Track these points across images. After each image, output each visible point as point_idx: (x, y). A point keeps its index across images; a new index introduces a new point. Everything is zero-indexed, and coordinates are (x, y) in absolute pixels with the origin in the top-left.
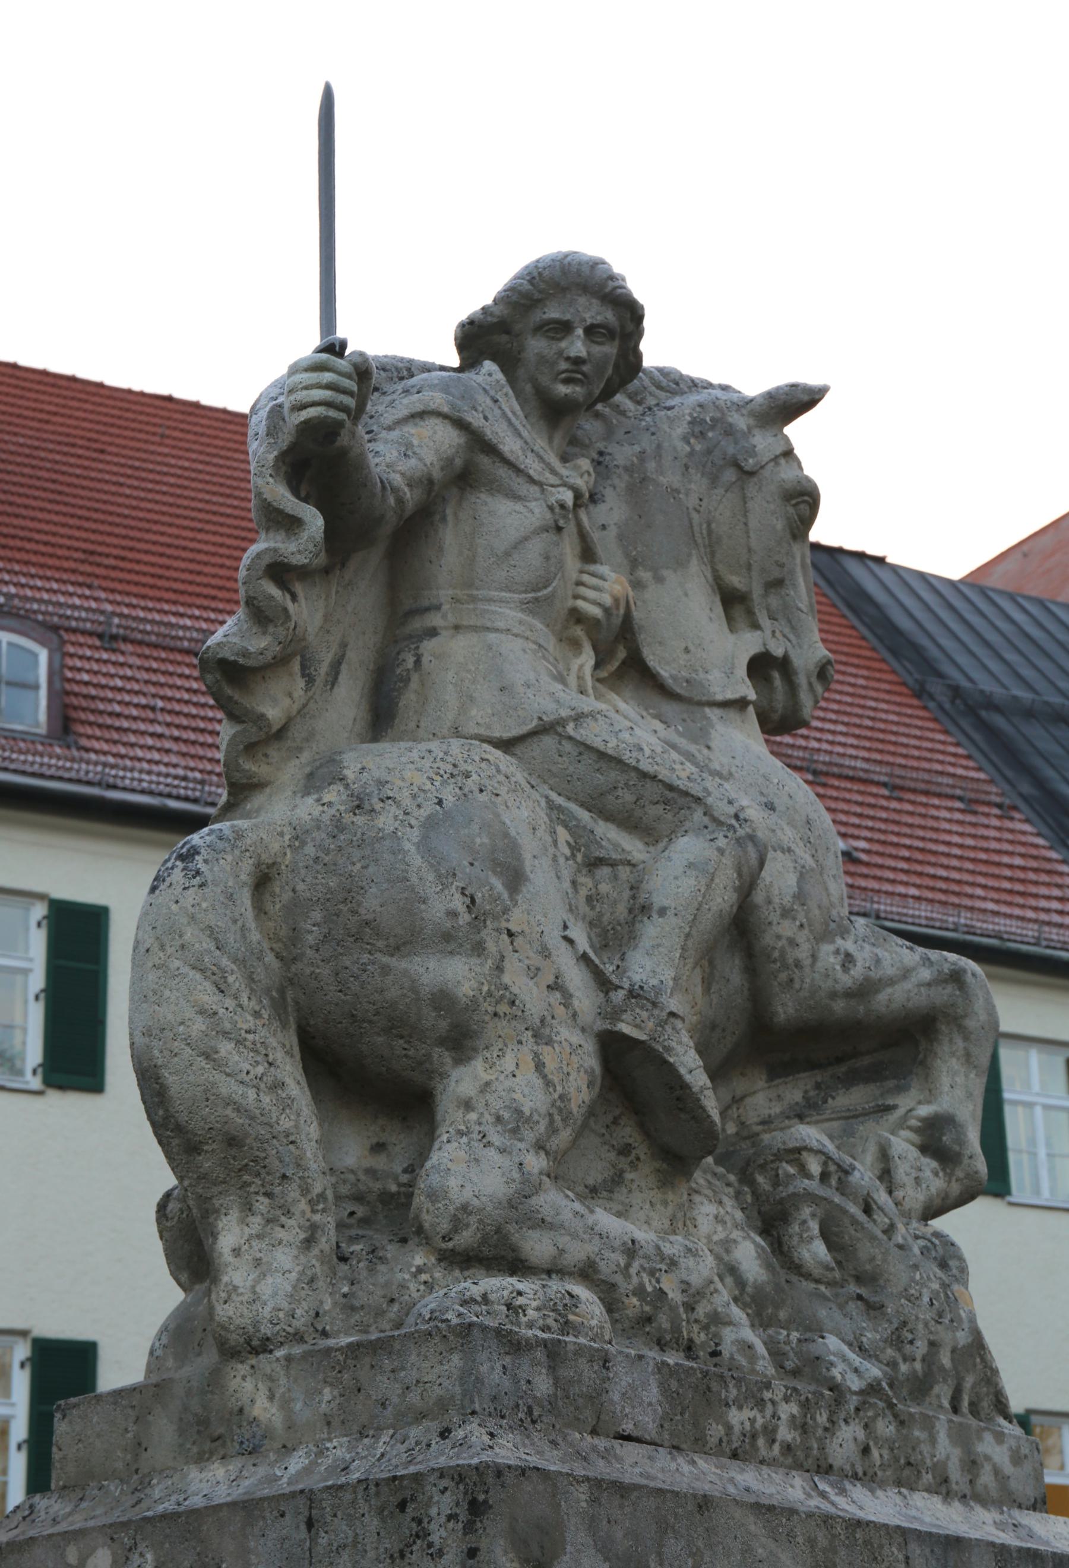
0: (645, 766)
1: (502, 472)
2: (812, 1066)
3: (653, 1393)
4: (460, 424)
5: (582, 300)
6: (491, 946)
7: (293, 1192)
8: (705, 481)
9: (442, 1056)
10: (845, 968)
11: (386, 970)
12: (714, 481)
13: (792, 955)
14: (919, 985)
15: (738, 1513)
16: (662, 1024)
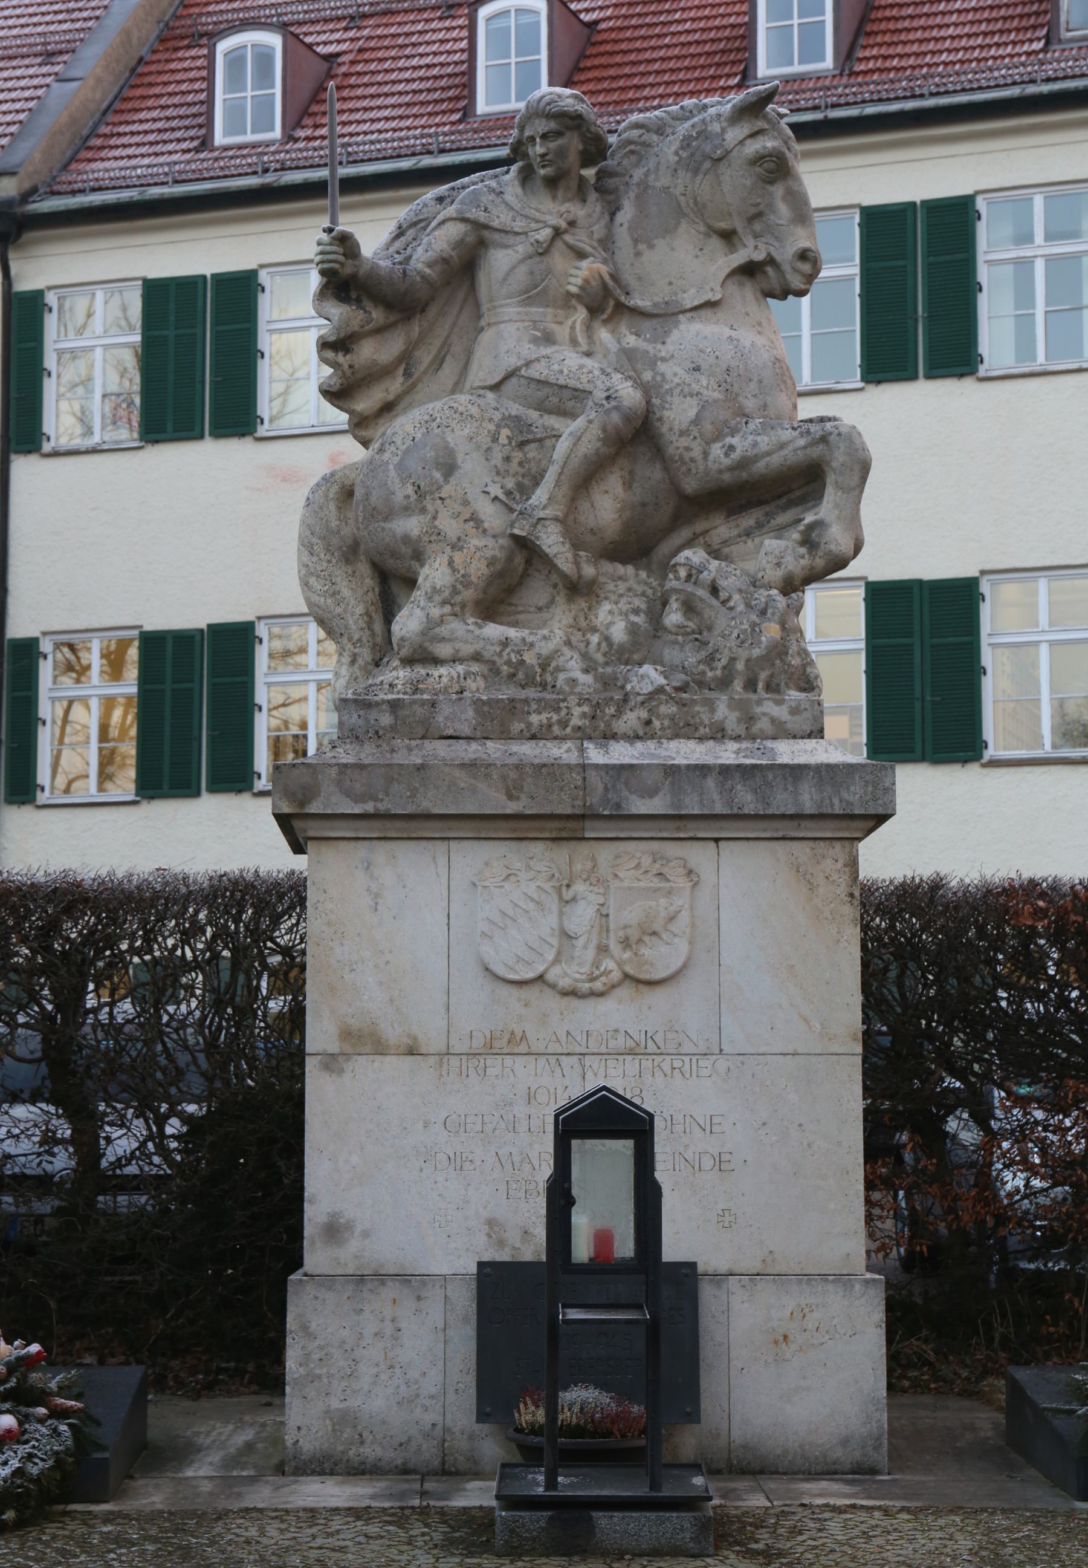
0: (561, 382)
1: (496, 236)
2: (760, 503)
3: (470, 713)
5: (537, 121)
6: (430, 508)
7: (345, 640)
8: (689, 174)
9: (415, 564)
10: (726, 455)
11: (383, 529)
12: (696, 171)
13: (687, 456)
14: (795, 450)
15: (447, 769)
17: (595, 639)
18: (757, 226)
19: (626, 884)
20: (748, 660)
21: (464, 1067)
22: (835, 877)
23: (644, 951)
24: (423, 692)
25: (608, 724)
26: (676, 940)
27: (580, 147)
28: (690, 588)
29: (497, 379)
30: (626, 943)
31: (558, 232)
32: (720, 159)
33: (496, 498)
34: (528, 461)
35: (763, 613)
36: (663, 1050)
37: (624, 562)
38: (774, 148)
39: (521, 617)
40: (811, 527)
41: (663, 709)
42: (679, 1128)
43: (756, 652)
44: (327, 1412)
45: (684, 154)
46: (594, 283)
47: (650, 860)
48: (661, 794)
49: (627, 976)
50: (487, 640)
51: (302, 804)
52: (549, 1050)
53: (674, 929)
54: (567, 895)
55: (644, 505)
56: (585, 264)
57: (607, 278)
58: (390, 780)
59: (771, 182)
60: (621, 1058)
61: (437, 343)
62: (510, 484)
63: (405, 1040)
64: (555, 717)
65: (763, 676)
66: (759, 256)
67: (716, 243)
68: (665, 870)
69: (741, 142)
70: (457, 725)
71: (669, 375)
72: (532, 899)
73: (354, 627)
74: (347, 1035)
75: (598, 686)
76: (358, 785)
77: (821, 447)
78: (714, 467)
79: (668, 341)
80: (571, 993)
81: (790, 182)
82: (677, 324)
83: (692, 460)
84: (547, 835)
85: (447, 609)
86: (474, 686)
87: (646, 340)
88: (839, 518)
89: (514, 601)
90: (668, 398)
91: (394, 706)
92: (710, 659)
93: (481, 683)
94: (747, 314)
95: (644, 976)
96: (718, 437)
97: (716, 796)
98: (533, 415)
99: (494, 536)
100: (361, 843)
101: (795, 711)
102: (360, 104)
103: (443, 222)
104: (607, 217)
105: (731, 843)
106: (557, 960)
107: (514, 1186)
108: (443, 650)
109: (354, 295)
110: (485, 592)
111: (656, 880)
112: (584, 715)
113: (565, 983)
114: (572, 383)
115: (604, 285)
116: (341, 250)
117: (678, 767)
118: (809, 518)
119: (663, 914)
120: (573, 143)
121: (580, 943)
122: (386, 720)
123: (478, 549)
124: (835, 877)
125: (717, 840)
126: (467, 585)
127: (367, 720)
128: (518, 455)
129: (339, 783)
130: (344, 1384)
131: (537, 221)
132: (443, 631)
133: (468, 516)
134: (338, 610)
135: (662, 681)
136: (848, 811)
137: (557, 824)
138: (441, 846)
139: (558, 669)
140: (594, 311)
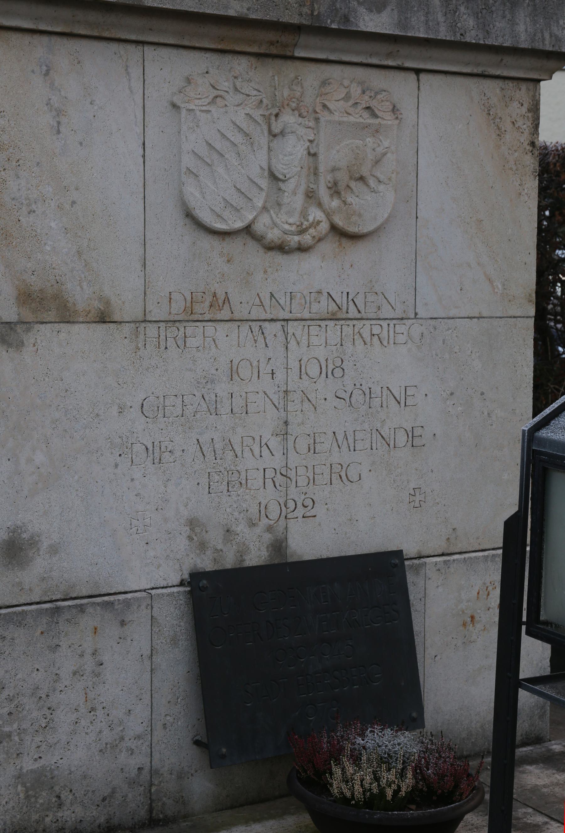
19: (336, 117)
21: (162, 337)
26: (381, 187)
36: (364, 315)
42: (376, 402)
44: (19, 776)
47: (359, 91)
48: (389, 9)
49: (334, 228)
52: (253, 316)
53: (379, 175)
60: (323, 323)
63: (96, 304)
68: (373, 104)
72: (240, 129)
84: (255, 49)
95: (352, 229)
97: (441, 19)
100: (37, 39)
107: (217, 478)
111: (366, 114)
113: (273, 235)
119: (371, 156)
125: (418, 72)
130: (38, 739)
137: (271, 36)
138: (134, 52)
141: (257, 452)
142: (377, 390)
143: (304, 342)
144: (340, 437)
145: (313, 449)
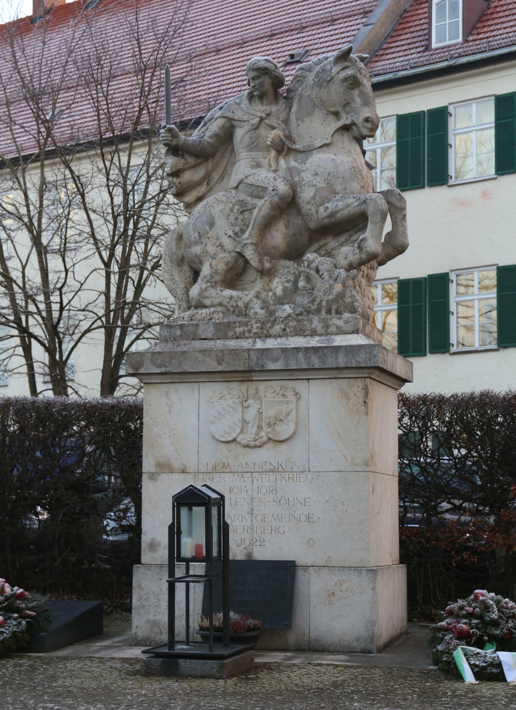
0: (258, 184)
2: (347, 231)
3: (212, 328)
4: (224, 117)
6: (204, 242)
10: (325, 211)
12: (321, 87)
13: (310, 213)
15: (194, 353)
16: (243, 247)
17: (270, 294)
18: (348, 109)
19: (269, 399)
20: (327, 301)
22: (358, 394)
23: (277, 428)
24: (194, 320)
25: (268, 331)
26: (290, 423)
27: (270, 81)
28: (308, 270)
29: (236, 185)
30: (269, 425)
31: (262, 119)
32: (329, 81)
33: (230, 236)
34: (245, 219)
35: (336, 280)
37: (290, 260)
38: (351, 74)
39: (246, 286)
40: (362, 241)
41: (291, 324)
43: (331, 297)
44: (148, 621)
45: (316, 80)
46: (277, 140)
47: (279, 389)
49: (270, 439)
50: (224, 297)
51: (137, 369)
52: (239, 471)
54: (245, 405)
55: (295, 235)
56: (273, 132)
57: (282, 137)
58: (171, 358)
59: (352, 89)
60: (268, 474)
61: (221, 170)
62: (237, 229)
64: (246, 329)
65: (334, 307)
66: (348, 122)
67: (331, 117)
68: (285, 393)
69: (338, 73)
70: (207, 334)
71: (305, 178)
73: (179, 293)
74: (159, 465)
75: (267, 314)
76: (159, 361)
77: (364, 205)
78: (320, 217)
79: (307, 162)
80: (247, 446)
81: (361, 88)
82: (312, 154)
83: (312, 214)
84: (237, 379)
85: (209, 284)
86: (217, 317)
87: (298, 163)
88: (372, 236)
89: (243, 279)
90: (303, 188)
91: (182, 326)
92: (314, 300)
93: (221, 315)
94: (344, 148)
95: (276, 439)
96: (322, 203)
97: (303, 361)
98: (249, 199)
99: (229, 252)
100: (164, 385)
101: (346, 322)
102: (500, 21)
103: (217, 119)
104: (288, 110)
105: (314, 381)
106: (242, 431)
108: (207, 302)
109: (181, 153)
110: (225, 276)
111: (281, 397)
112: (258, 327)
113: (244, 442)
114: (262, 184)
115: (282, 141)
116: (170, 135)
117: (287, 349)
118: (361, 237)
119: (285, 412)
120: (267, 81)
121: (250, 425)
122: (178, 332)
123: (222, 258)
124: (358, 394)
126: (217, 274)
127: (171, 333)
128: (241, 217)
129: (151, 360)
130: (155, 609)
131: (253, 115)
132: (207, 294)
133: (218, 244)
134: (174, 286)
135: (291, 311)
136: (358, 366)
138: (196, 385)
139: (251, 308)
140: (279, 152)
141: (240, 519)
142: (291, 499)
143: (260, 480)
144: (275, 516)
145: (263, 520)
